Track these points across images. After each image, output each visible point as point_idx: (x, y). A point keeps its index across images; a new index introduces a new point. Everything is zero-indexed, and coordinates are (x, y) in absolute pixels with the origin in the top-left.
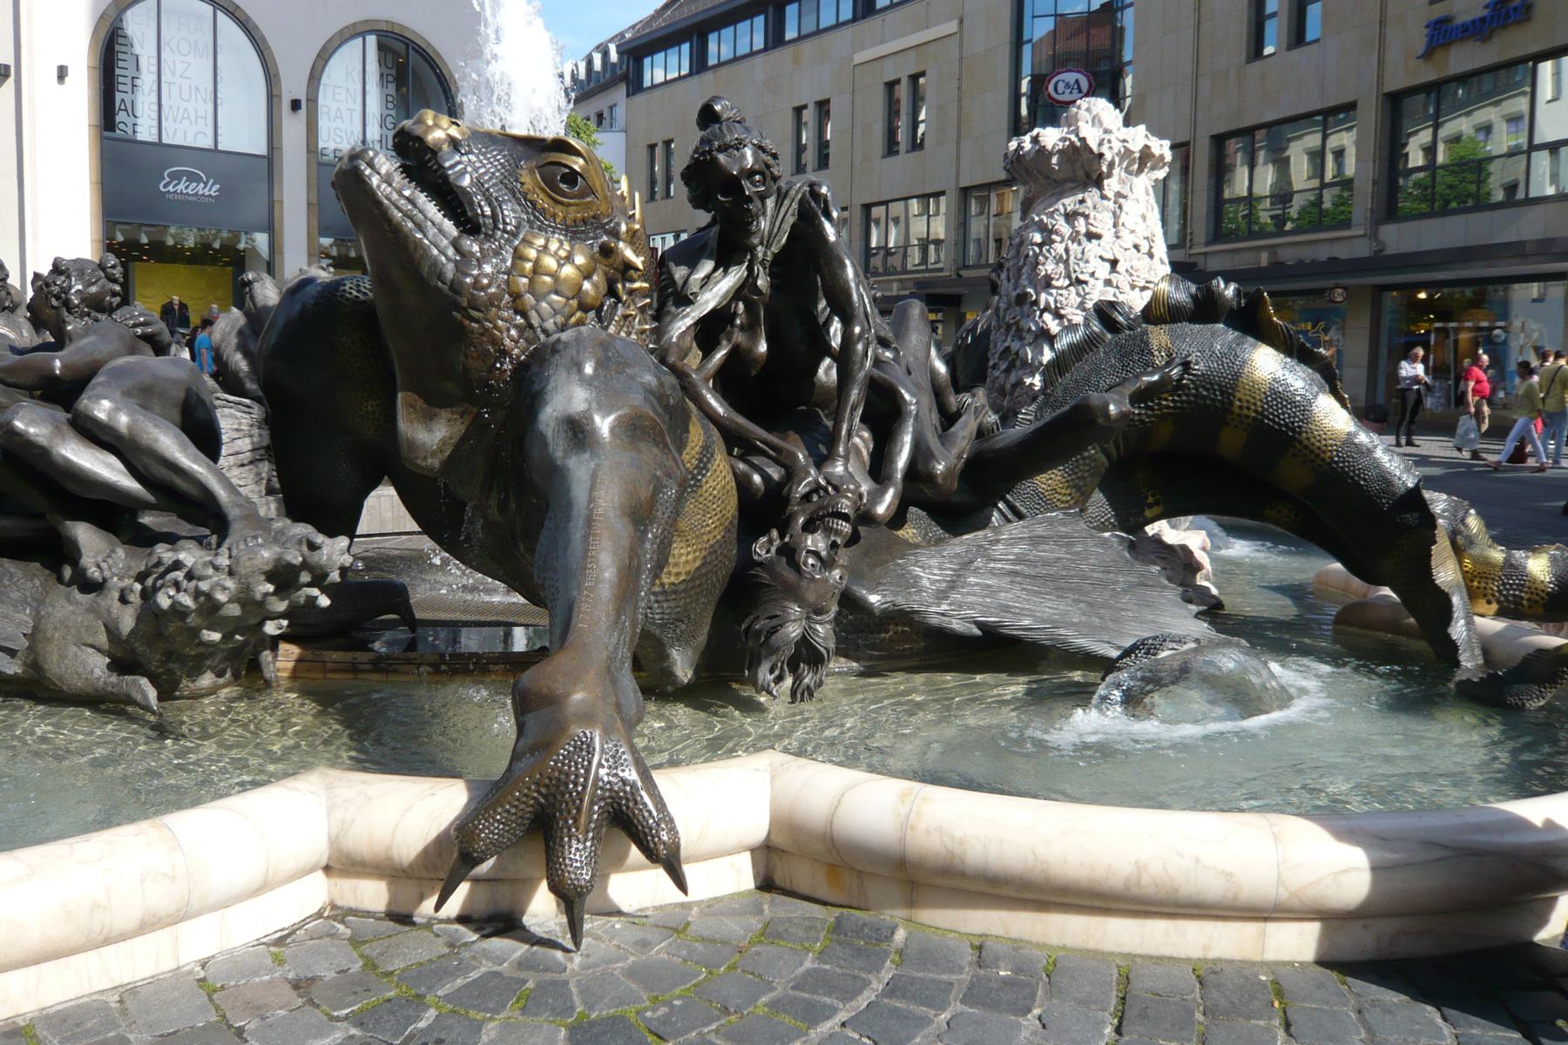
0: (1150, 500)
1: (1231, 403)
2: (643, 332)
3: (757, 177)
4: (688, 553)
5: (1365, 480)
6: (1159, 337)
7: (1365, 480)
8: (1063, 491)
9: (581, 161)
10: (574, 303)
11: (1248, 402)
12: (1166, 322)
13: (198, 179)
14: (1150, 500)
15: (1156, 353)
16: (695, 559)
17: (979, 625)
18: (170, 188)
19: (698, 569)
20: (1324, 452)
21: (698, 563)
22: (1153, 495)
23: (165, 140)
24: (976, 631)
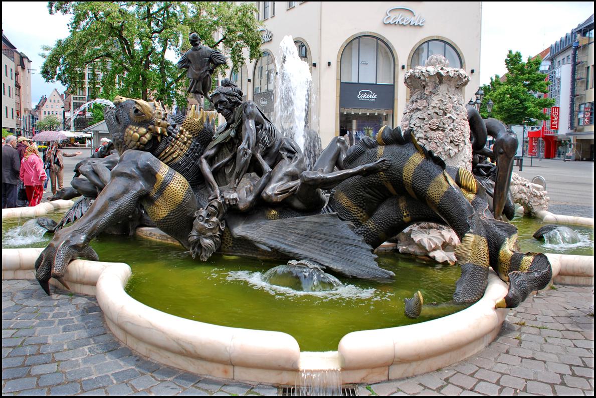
0: (405, 214)
1: (402, 177)
2: (182, 150)
3: (225, 103)
4: (162, 212)
5: (451, 212)
6: (381, 150)
7: (451, 212)
8: (353, 207)
9: (140, 107)
10: (139, 143)
11: (407, 177)
12: (384, 145)
13: (370, 93)
14: (405, 214)
15: (378, 156)
16: (165, 214)
17: (271, 248)
18: (361, 97)
19: (166, 216)
20: (436, 199)
21: (166, 215)
22: (406, 212)
23: (360, 82)
24: (269, 250)
